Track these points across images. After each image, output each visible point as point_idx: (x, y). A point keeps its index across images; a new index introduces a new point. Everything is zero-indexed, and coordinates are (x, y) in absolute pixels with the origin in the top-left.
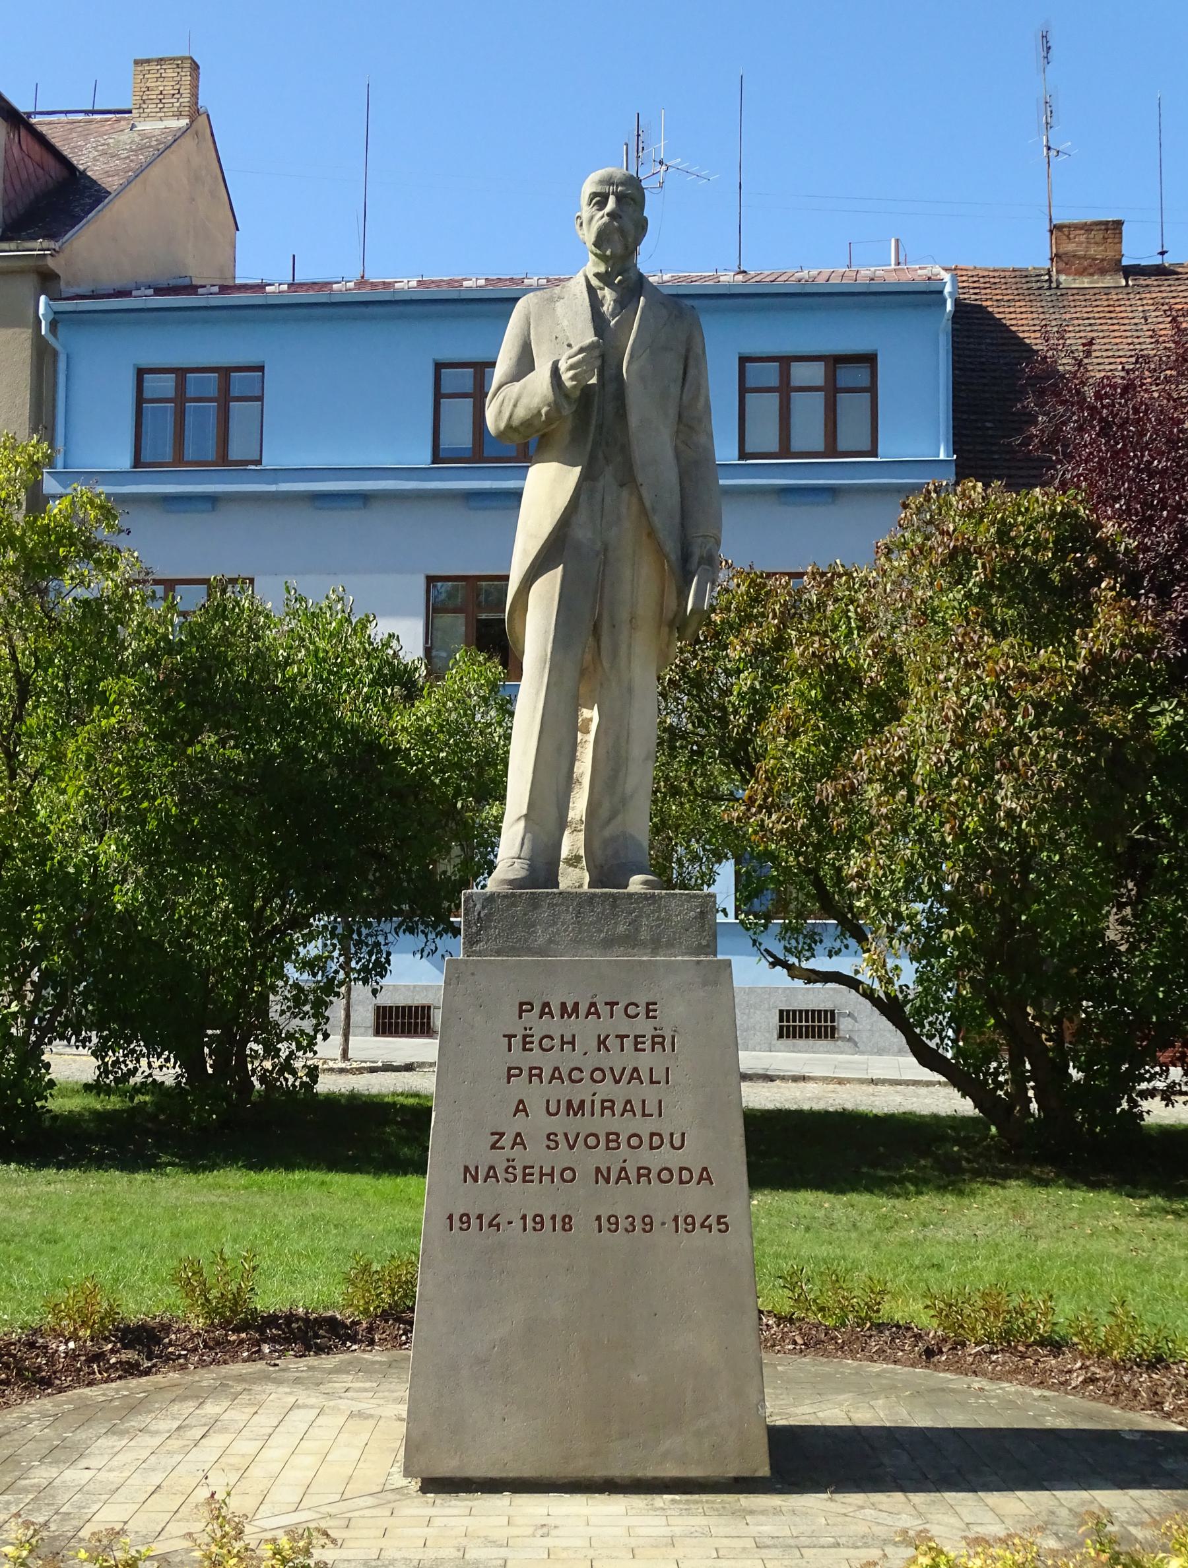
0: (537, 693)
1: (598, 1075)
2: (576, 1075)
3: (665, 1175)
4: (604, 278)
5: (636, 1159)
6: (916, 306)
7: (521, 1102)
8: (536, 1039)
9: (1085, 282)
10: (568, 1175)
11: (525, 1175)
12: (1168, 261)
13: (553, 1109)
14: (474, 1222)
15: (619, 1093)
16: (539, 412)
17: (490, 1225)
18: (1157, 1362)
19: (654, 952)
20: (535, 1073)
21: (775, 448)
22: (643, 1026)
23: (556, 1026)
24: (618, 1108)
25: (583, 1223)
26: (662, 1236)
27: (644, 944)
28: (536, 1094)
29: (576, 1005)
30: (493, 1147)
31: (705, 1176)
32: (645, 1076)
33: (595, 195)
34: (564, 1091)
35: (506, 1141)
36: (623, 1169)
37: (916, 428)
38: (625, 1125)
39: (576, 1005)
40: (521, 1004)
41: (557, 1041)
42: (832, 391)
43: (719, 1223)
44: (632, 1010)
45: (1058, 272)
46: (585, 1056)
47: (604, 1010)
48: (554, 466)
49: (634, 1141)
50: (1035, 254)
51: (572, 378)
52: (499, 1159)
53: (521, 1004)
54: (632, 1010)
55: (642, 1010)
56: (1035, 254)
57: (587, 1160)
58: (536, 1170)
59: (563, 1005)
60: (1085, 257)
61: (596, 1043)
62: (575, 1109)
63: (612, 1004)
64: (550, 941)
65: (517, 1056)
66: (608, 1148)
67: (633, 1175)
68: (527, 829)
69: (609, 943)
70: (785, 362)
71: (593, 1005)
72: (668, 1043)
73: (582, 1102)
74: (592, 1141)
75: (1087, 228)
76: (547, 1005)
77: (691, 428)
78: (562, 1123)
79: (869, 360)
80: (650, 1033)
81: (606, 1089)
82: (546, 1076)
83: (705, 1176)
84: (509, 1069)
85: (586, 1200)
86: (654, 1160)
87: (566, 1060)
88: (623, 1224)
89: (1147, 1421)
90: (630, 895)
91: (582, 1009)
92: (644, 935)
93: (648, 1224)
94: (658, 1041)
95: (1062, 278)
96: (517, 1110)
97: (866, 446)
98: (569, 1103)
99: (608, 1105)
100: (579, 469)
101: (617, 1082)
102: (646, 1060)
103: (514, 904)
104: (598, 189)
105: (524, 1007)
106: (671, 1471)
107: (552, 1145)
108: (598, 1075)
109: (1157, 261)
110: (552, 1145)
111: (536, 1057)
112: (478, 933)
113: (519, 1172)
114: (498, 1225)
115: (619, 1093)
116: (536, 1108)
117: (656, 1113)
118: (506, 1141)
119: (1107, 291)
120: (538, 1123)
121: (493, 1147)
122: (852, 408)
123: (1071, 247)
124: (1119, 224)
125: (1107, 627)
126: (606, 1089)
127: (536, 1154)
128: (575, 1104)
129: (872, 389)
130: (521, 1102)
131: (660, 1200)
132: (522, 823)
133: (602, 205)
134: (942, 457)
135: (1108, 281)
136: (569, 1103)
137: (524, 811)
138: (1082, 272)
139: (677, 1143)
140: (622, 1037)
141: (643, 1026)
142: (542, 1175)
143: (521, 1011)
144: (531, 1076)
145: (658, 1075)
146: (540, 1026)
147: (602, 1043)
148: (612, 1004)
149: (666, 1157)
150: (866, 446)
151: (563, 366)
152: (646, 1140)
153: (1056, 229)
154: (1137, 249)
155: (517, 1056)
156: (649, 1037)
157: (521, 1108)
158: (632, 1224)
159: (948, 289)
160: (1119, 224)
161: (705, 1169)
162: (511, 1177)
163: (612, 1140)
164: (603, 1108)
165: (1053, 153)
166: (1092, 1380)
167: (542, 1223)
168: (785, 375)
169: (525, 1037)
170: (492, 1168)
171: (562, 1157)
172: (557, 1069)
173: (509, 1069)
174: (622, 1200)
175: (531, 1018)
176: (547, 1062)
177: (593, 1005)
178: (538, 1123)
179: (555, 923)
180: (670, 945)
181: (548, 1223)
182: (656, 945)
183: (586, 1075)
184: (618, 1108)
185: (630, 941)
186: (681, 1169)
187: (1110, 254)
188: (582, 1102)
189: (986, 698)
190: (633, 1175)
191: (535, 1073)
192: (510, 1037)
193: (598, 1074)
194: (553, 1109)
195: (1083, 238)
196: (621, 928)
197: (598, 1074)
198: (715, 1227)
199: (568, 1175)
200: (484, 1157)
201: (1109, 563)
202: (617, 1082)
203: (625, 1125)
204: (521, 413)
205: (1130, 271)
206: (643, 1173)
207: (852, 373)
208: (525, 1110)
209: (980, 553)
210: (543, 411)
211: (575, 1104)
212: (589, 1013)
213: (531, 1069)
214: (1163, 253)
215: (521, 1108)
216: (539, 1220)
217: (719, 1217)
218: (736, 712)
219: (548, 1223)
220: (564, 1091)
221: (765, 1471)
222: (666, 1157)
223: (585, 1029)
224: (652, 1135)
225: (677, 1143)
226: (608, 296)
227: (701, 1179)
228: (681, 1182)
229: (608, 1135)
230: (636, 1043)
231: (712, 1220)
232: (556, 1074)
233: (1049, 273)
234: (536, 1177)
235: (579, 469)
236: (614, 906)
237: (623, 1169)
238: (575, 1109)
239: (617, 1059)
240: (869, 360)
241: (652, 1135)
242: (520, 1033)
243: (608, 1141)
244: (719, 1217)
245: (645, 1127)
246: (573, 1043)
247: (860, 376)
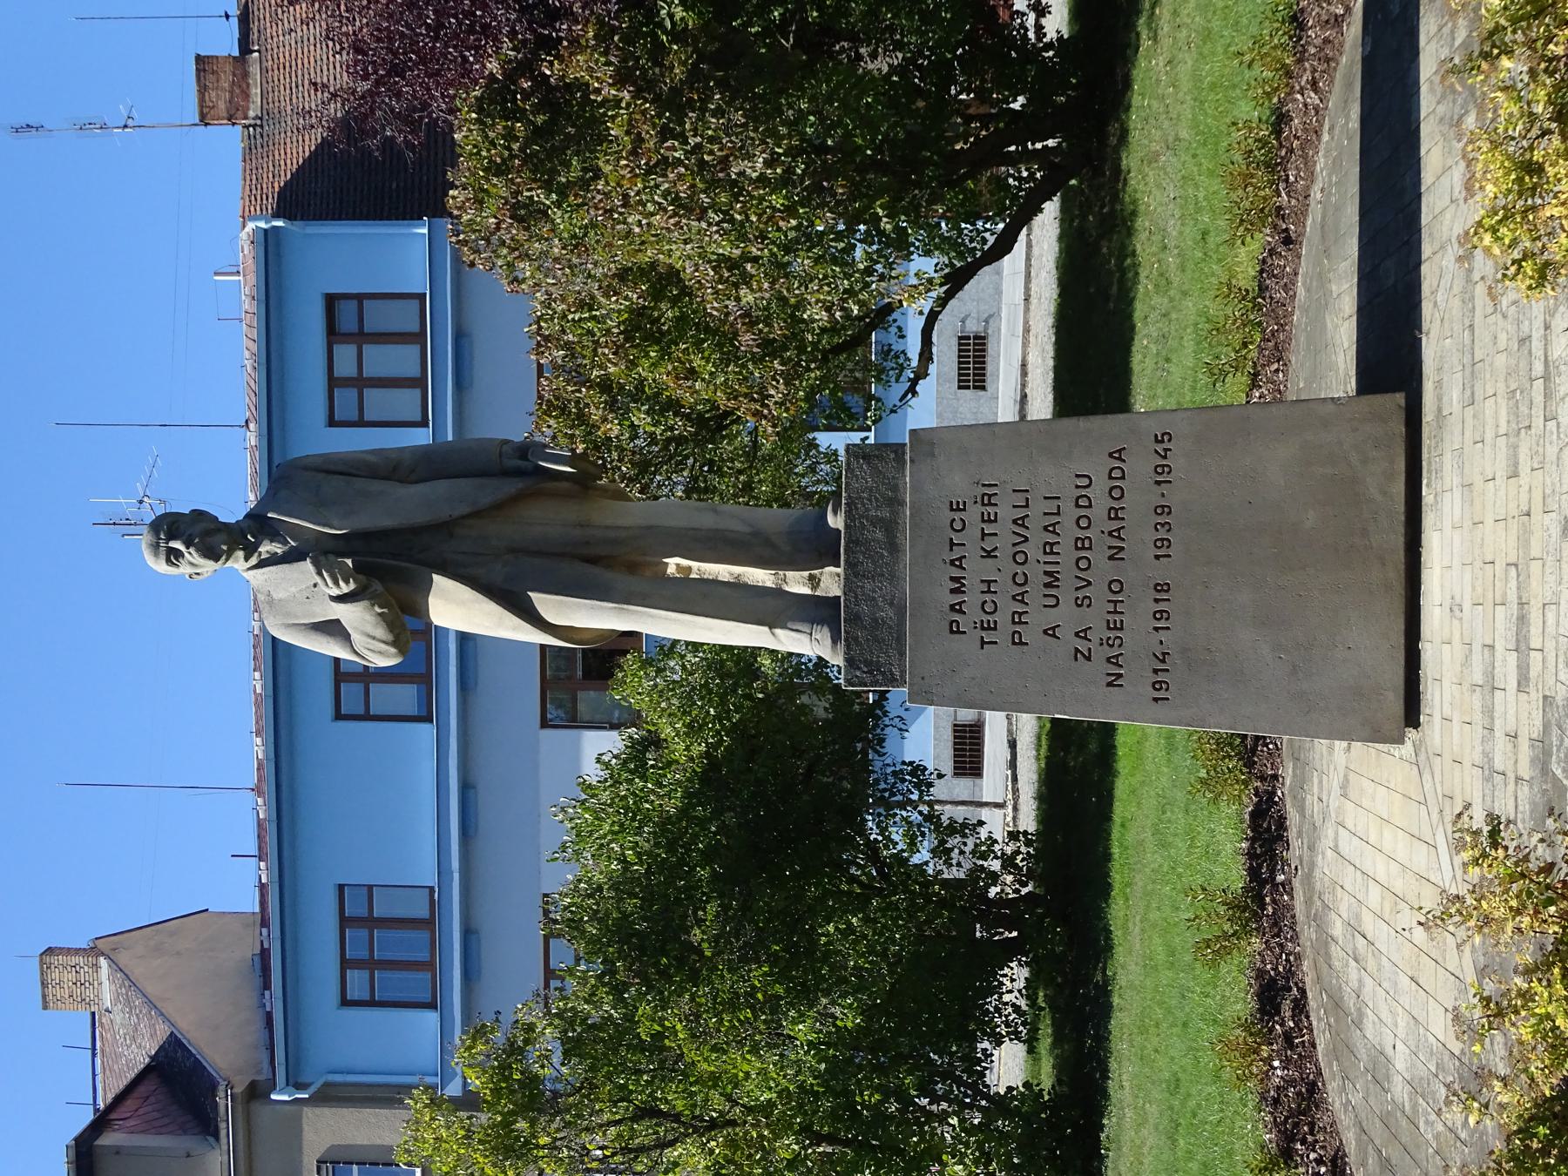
0: (652, 616)
1: (1020, 558)
2: (1020, 580)
3: (1116, 494)
4: (250, 550)
5: (1101, 522)
6: (279, 255)
7: (1045, 632)
8: (985, 618)
9: (256, 91)
11: (1115, 628)
12: (234, 11)
13: (1052, 602)
15: (1037, 537)
16: (380, 614)
17: (1163, 661)
18: (1297, 21)
19: (902, 503)
20: (1018, 619)
21: (417, 392)
22: (973, 514)
23: (972, 598)
24: (1051, 539)
26: (1175, 497)
27: (895, 513)
28: (1038, 618)
29: (952, 579)
30: (1088, 659)
31: (1117, 455)
32: (1020, 513)
33: (168, 561)
34: (1035, 591)
35: (1082, 646)
36: (1110, 534)
37: (399, 256)
39: (952, 579)
40: (952, 632)
41: (987, 597)
42: (362, 337)
43: (1162, 441)
44: (957, 526)
45: (246, 118)
46: (1001, 571)
48: (431, 600)
49: (1084, 523)
50: (229, 140)
51: (347, 582)
52: (1100, 653)
53: (952, 632)
54: (957, 526)
55: (957, 516)
56: (229, 140)
57: (1102, 569)
58: (1110, 617)
59: (953, 591)
60: (231, 92)
61: (990, 560)
62: (1052, 580)
63: (952, 544)
64: (891, 604)
65: (1002, 636)
67: (1115, 525)
68: (784, 627)
69: (894, 547)
70: (333, 382)
71: (952, 562)
73: (1046, 573)
74: (1083, 564)
75: (203, 90)
76: (952, 607)
77: (395, 468)
79: (331, 301)
80: (979, 508)
81: (1033, 550)
83: (1117, 455)
84: (1014, 643)
85: (1141, 569)
86: (1101, 504)
87: (1005, 588)
89: (1353, 30)
90: (847, 526)
91: (957, 573)
92: (885, 513)
93: (1163, 510)
94: (988, 500)
95: (251, 114)
96: (1054, 636)
97: (415, 303)
98: (1047, 585)
100: (435, 576)
101: (1027, 539)
102: (1005, 512)
103: (856, 639)
104: (163, 557)
106: (1399, 487)
107: (1087, 602)
108: (1020, 558)
109: (234, 21)
110: (1087, 602)
111: (1002, 618)
112: (883, 673)
113: (1112, 634)
114: (1164, 654)
115: (1037, 537)
116: (1053, 617)
117: (1056, 502)
118: (1082, 646)
119: (264, 71)
120: (1066, 616)
121: (1088, 659)
122: (379, 318)
123: (222, 105)
124: (199, 58)
125: (590, 69)
126: (1033, 550)
127: (1095, 618)
129: (360, 298)
130: (1045, 632)
131: (1139, 501)
132: (778, 631)
133: (178, 554)
134: (425, 231)
135: (255, 70)
136: (1047, 585)
137: (766, 629)
138: (246, 95)
139: (1085, 482)
140: (984, 535)
141: (973, 514)
142: (1116, 612)
143: (958, 632)
144: (1020, 623)
146: (973, 614)
147: (989, 554)
148: (952, 544)
149: (1098, 492)
150: (415, 303)
151: (335, 592)
152: (1083, 512)
153: (204, 120)
154: (225, 42)
155: (1002, 636)
156: (983, 509)
157: (1051, 632)
158: (1163, 525)
159: (263, 225)
160: (199, 58)
161: (1111, 455)
162: (1117, 642)
163: (1081, 544)
164: (1052, 553)
165: (130, 122)
166: (1314, 84)
167: (1161, 612)
168: (347, 382)
169: (983, 628)
170: (1108, 660)
171: (1098, 592)
172: (1014, 597)
173: (1014, 643)
174: (1140, 537)
176: (1007, 607)
177: (952, 562)
178: (1066, 616)
179: (874, 599)
180: (895, 489)
181: (1162, 606)
182: (895, 502)
184: (1051, 539)
185: (891, 527)
186: (1110, 477)
187: (228, 68)
189: (657, 186)
190: (1115, 525)
191: (1018, 619)
192: (983, 643)
194: (1052, 602)
195: (213, 94)
196: (879, 535)
201: (526, 67)
204: (381, 632)
205: (245, 48)
206: (1114, 514)
207: (345, 318)
208: (1053, 629)
209: (518, 193)
210: (379, 611)
212: (961, 567)
213: (1014, 622)
214: (227, 16)
215: (1051, 632)
216: (1159, 615)
217: (1157, 441)
218: (672, 429)
219: (1162, 606)
220: (1035, 591)
221: (1400, 398)
222: (1098, 492)
223: (976, 570)
224: (1077, 506)
225: (1085, 482)
226: (267, 548)
227: (1120, 459)
228: (1123, 478)
229: (1077, 548)
230: (989, 521)
232: (1019, 598)
233: (246, 127)
235: (435, 576)
236: (857, 542)
237: (1110, 534)
238: (1052, 580)
239: (1004, 540)
240: (331, 301)
241: (1077, 506)
243: (1083, 548)
244: (1157, 441)
245: (1070, 513)
246: (989, 582)
247: (347, 312)
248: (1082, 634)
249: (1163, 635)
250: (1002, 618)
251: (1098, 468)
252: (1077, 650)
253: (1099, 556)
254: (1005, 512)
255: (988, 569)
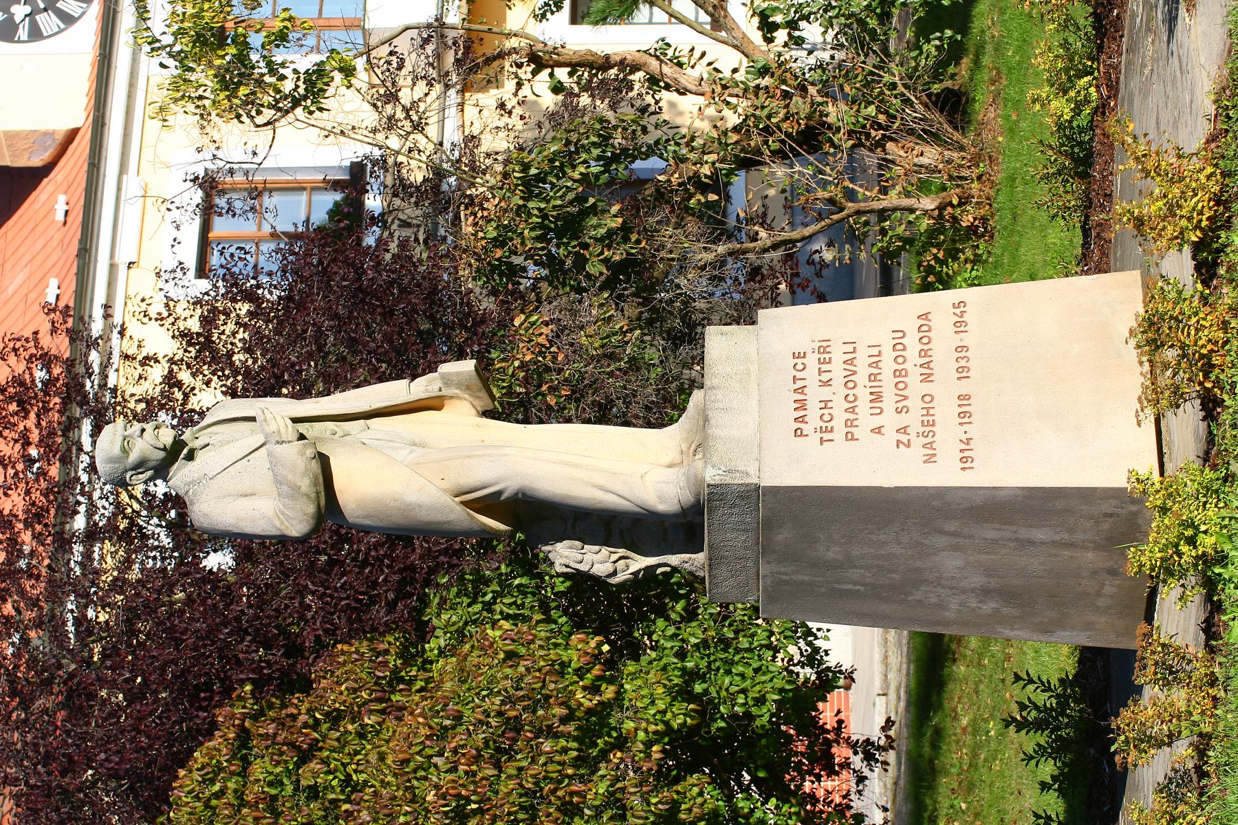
1: (851, 385)
2: (851, 398)
3: (925, 340)
8: (824, 425)
10: (927, 398)
14: (967, 454)
20: (849, 423)
22: (812, 360)
23: (813, 412)
25: (964, 387)
28: (865, 420)
30: (908, 446)
31: (925, 316)
35: (904, 438)
38: (888, 366)
41: (826, 411)
44: (800, 367)
46: (837, 393)
47: (800, 384)
52: (918, 442)
57: (916, 388)
58: (926, 418)
62: (877, 397)
66: (906, 376)
72: (825, 344)
73: (871, 393)
78: (889, 402)
80: (817, 356)
82: (852, 416)
85: (945, 391)
87: (839, 407)
88: (963, 363)
94: (823, 350)
96: (879, 432)
99: (873, 377)
102: (838, 356)
105: (798, 433)
108: (851, 385)
111: (838, 424)
114: (969, 439)
116: (877, 421)
117: (877, 349)
118: (904, 438)
120: (890, 420)
121: (908, 446)
126: (861, 378)
127: (913, 419)
128: (873, 397)
139: (901, 335)
140: (820, 372)
141: (812, 360)
145: (850, 348)
146: (813, 420)
147: (826, 384)
157: (878, 430)
171: (915, 403)
174: (944, 362)
175: (807, 429)
181: (964, 409)
183: (851, 392)
188: (871, 393)
193: (849, 383)
197: (849, 383)
198: (962, 309)
199: (927, 398)
200: (917, 449)
202: (855, 373)
203: (888, 366)
206: (923, 353)
211: (873, 397)
213: (846, 426)
215: (878, 430)
223: (815, 394)
225: (901, 335)
231: (958, 311)
232: (852, 410)
234: (931, 418)
238: (877, 397)
239: (837, 371)
242: (819, 435)
248: (903, 430)
249: (966, 427)
250: (838, 424)
251: (911, 326)
252: (899, 442)
253: (914, 378)
254: (838, 356)
255: (826, 393)
